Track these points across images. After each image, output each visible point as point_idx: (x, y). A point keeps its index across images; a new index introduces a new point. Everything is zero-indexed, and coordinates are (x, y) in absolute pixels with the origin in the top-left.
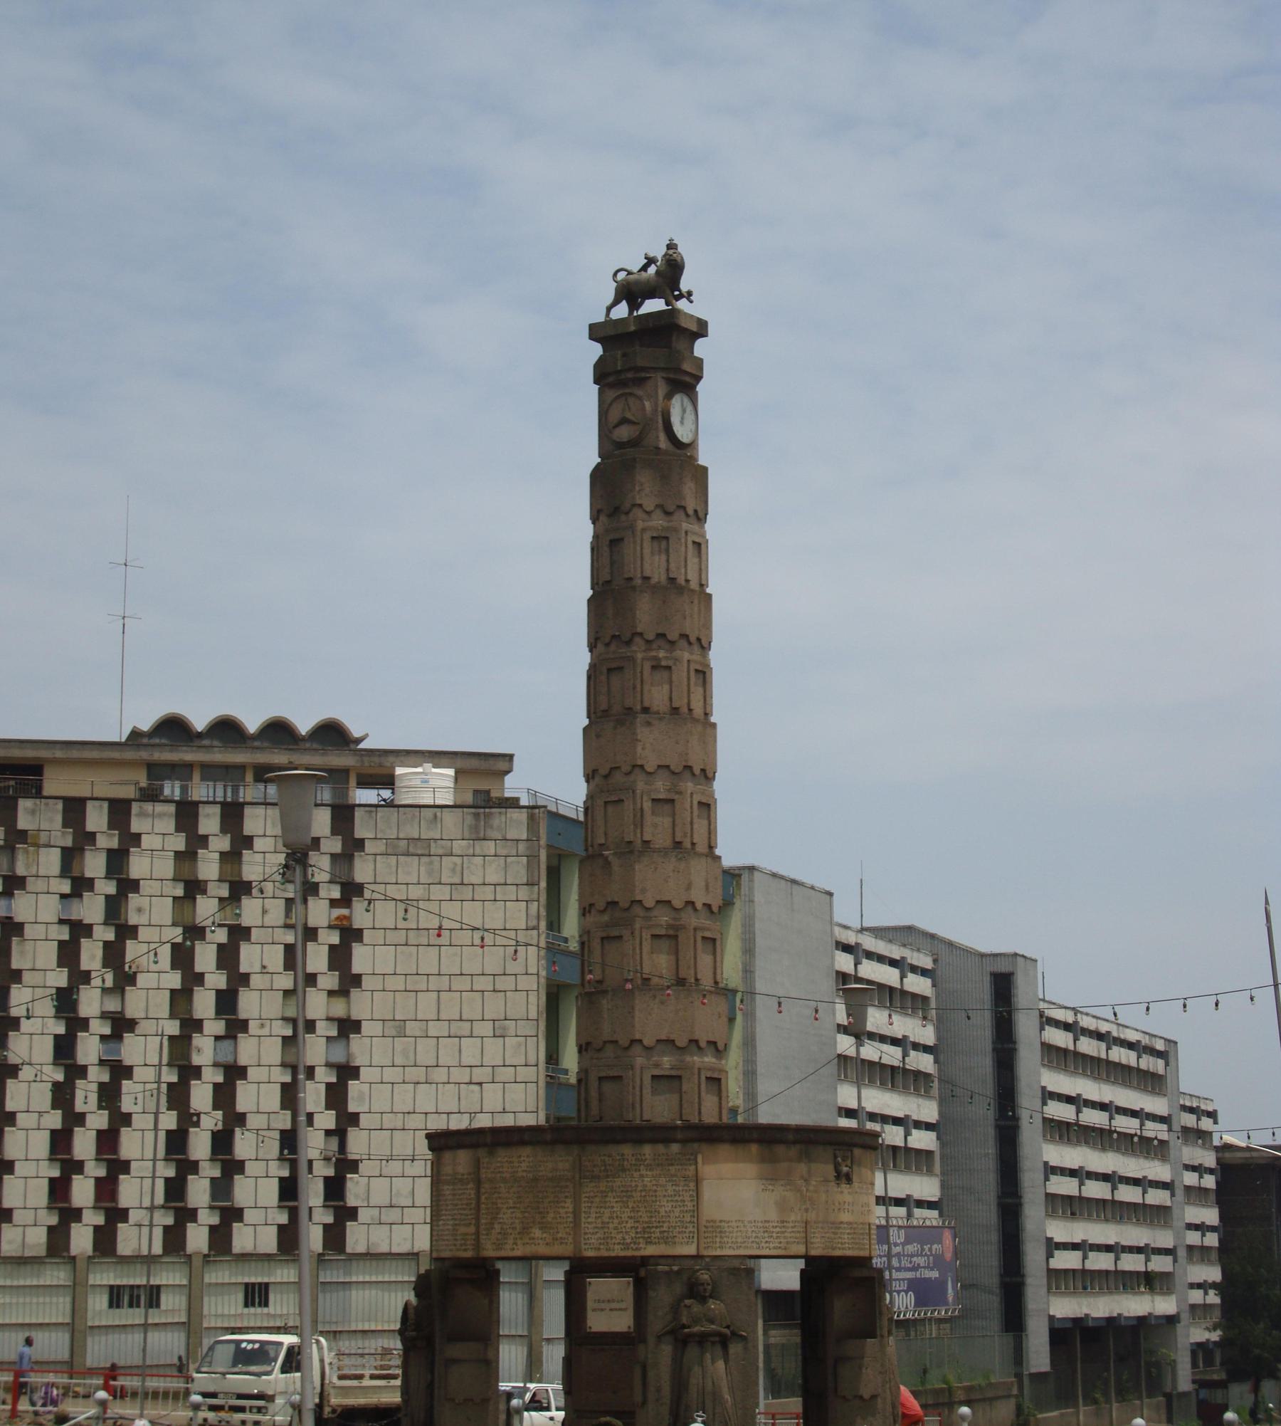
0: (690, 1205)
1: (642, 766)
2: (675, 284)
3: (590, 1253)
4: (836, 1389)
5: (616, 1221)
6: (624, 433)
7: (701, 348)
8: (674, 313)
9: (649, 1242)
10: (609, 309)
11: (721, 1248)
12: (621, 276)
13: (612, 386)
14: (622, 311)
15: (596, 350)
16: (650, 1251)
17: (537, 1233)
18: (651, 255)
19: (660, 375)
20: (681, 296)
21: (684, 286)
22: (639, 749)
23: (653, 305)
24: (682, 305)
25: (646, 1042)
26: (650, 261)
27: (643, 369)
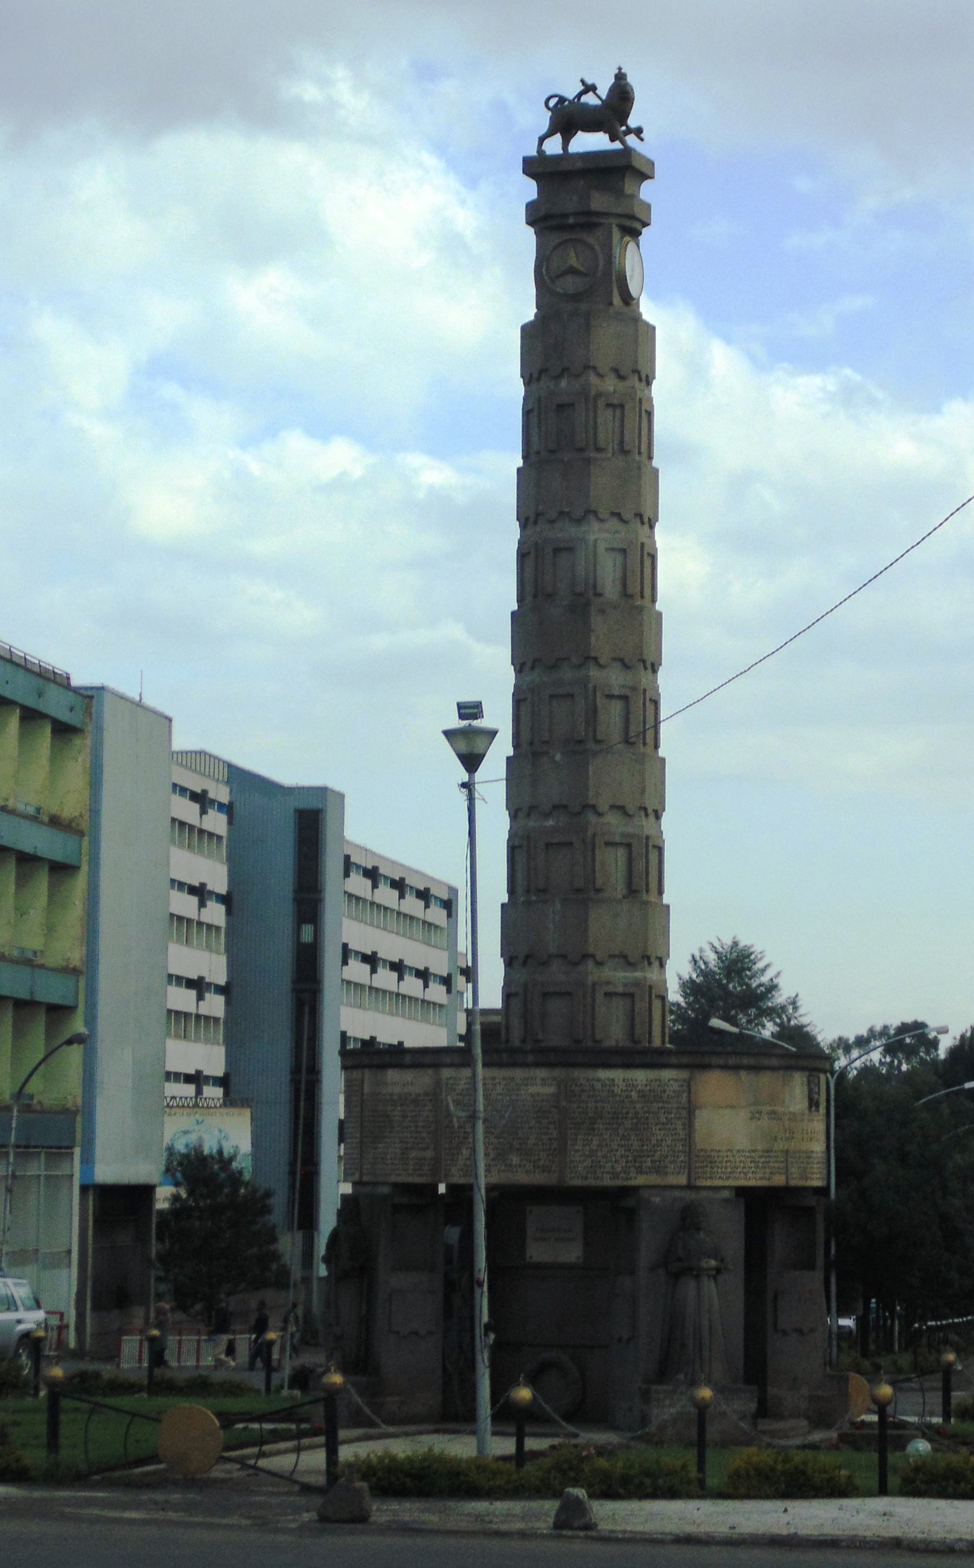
0: (682, 1134)
1: (595, 659)
2: (623, 115)
3: (578, 1182)
4: (775, 1325)
5: (605, 1149)
6: (570, 284)
7: (646, 191)
8: (627, 151)
9: (640, 1171)
10: (542, 140)
11: (711, 1178)
12: (552, 103)
13: (552, 229)
14: (554, 146)
15: (530, 190)
16: (640, 1180)
17: (515, 1159)
18: (589, 81)
19: (614, 221)
20: (629, 131)
21: (632, 122)
22: (593, 639)
23: (590, 142)
24: (631, 140)
25: (598, 958)
26: (589, 88)
27: (598, 214)
